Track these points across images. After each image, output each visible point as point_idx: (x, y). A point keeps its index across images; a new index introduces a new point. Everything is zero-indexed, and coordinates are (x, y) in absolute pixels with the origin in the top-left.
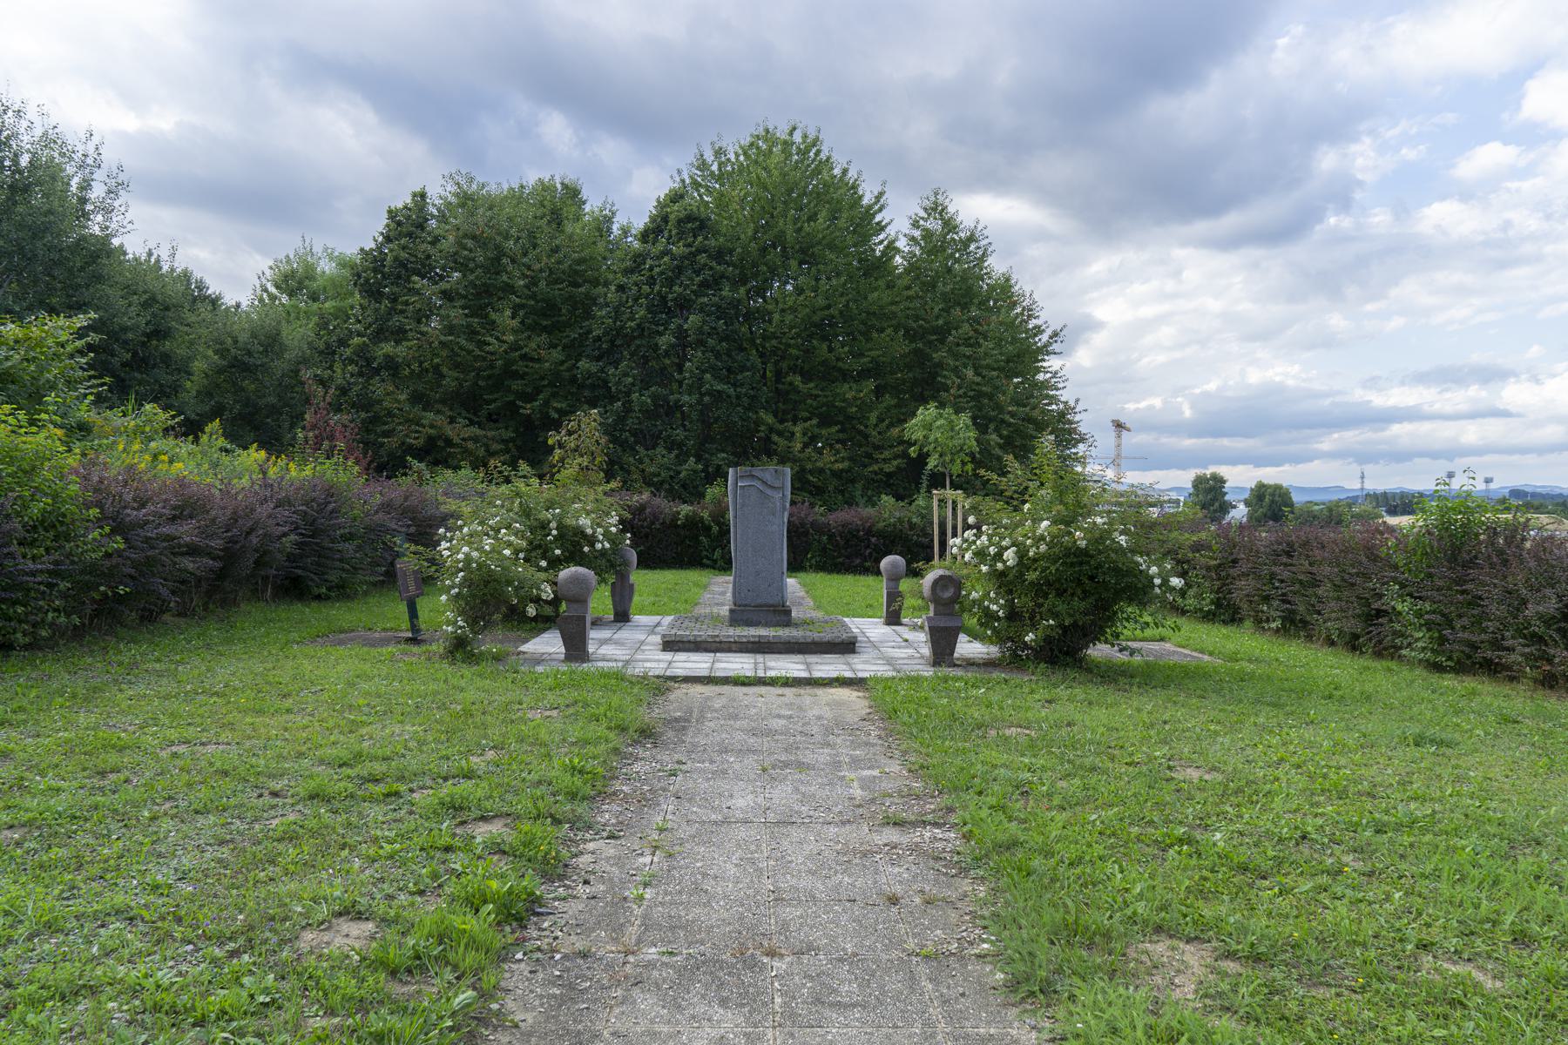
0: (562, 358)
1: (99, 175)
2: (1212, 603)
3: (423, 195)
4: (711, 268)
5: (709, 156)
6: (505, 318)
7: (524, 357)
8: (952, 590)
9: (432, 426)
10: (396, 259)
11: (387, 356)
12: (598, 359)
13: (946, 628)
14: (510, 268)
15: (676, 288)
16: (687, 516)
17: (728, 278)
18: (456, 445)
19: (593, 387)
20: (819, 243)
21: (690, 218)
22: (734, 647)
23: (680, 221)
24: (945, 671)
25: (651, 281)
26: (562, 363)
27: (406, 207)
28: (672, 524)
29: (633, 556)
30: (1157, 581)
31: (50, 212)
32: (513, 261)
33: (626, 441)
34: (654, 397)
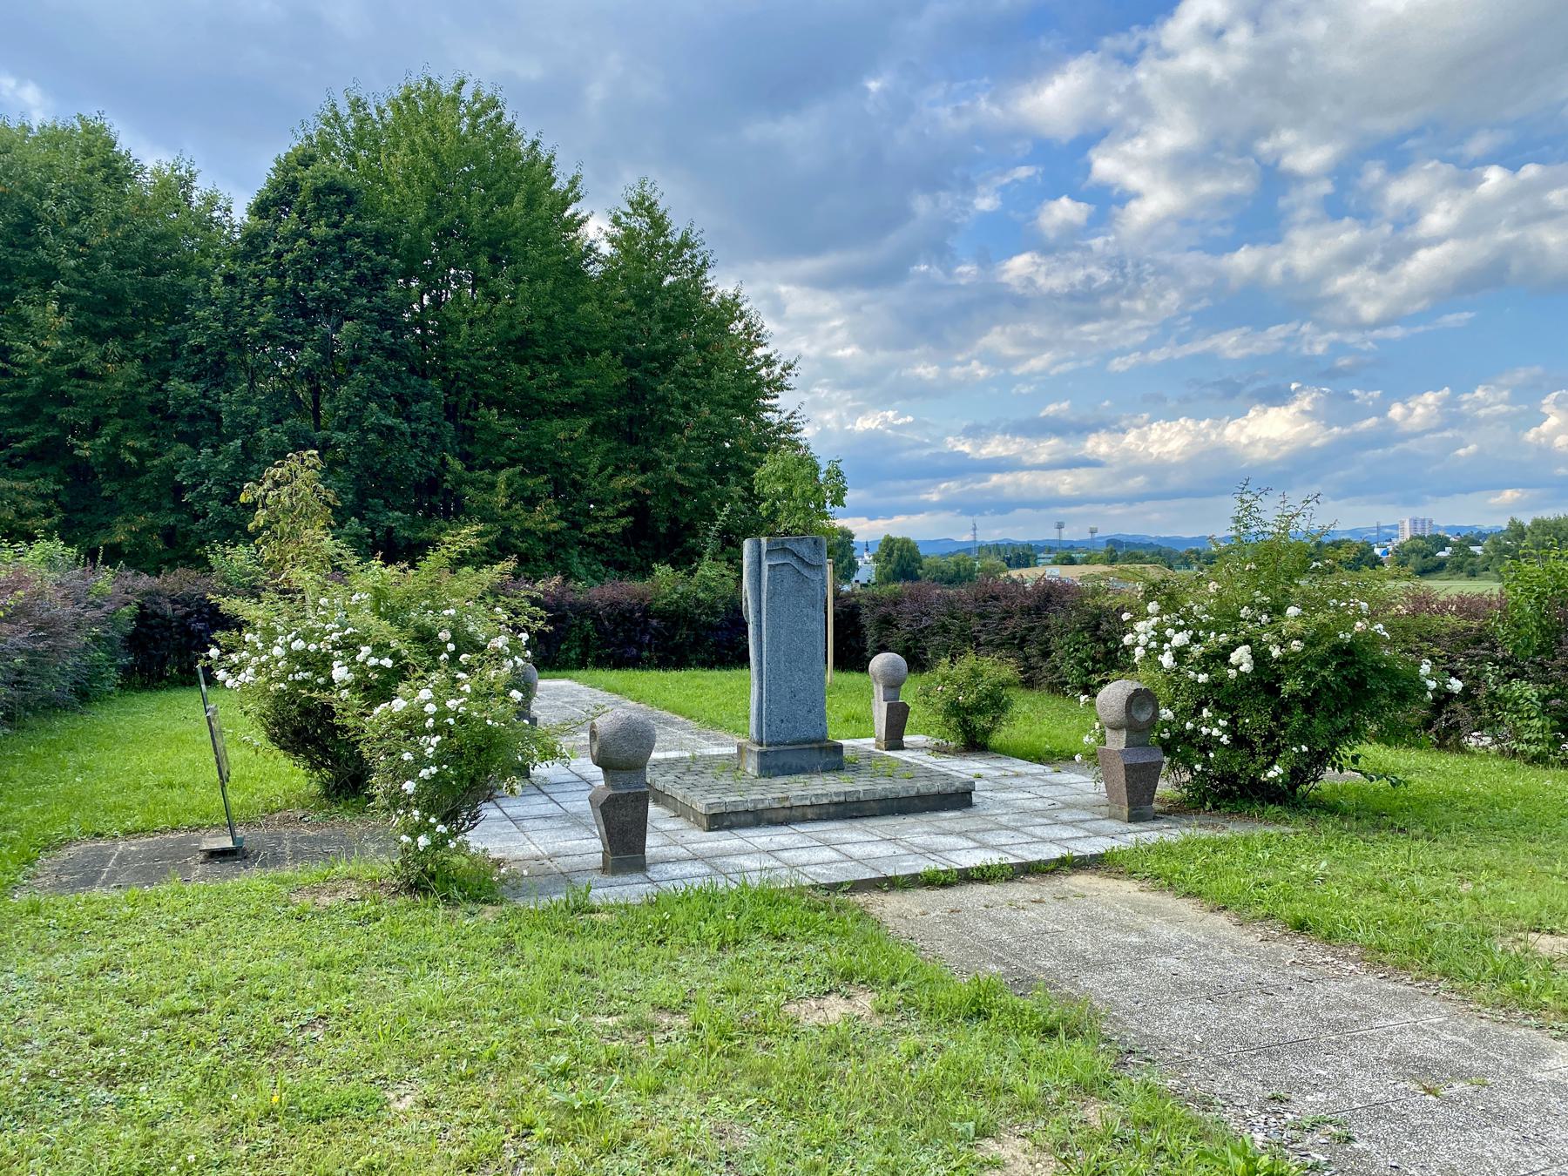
4: (369, 259)
5: (344, 110)
7: (82, 373)
12: (195, 379)
19: (192, 418)
20: (515, 235)
21: (332, 188)
22: (810, 813)
23: (317, 192)
26: (140, 383)
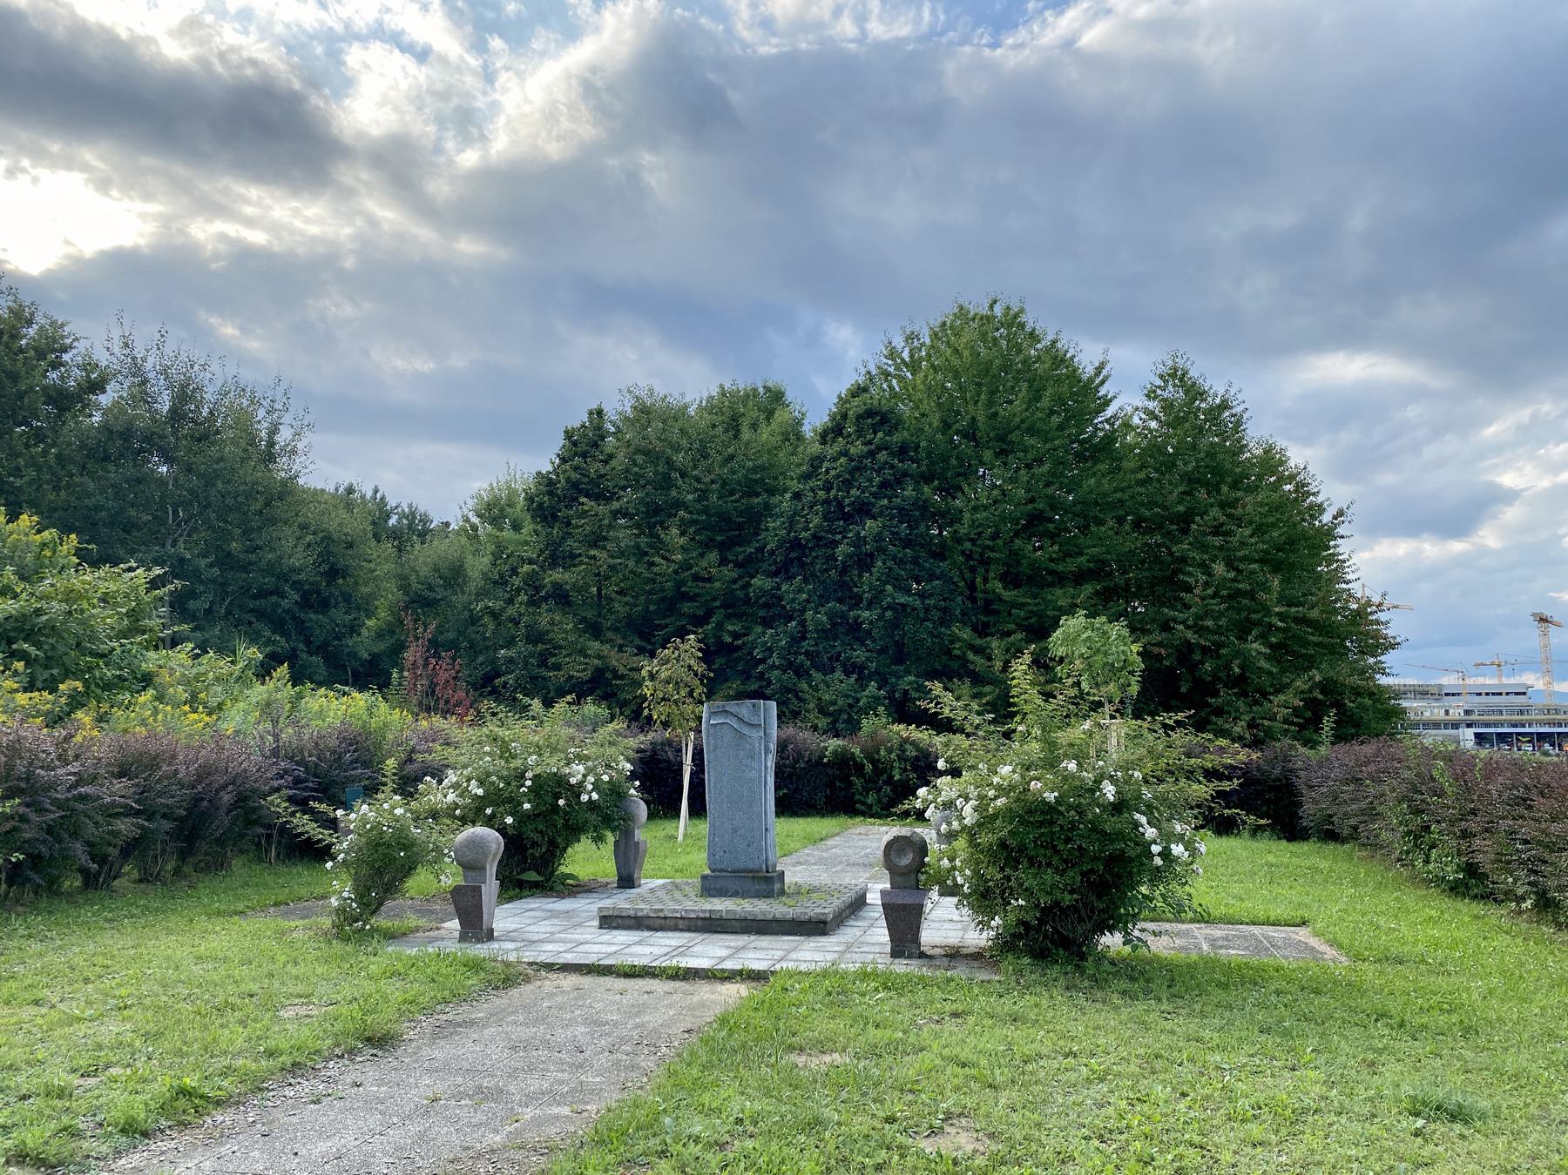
0: (735, 575)
1: (287, 418)
2: (1459, 869)
3: (600, 412)
4: (892, 467)
5: (899, 342)
6: (673, 536)
7: (696, 578)
8: (911, 856)
9: (599, 657)
10: (568, 480)
11: (554, 584)
12: (775, 574)
13: (904, 906)
14: (680, 482)
15: (853, 492)
16: (835, 752)
17: (911, 476)
18: (622, 677)
19: (767, 606)
20: (1018, 427)
21: (869, 413)
22: (681, 924)
23: (859, 417)
24: (902, 967)
25: (828, 487)
26: (734, 581)
27: (583, 426)
28: (817, 763)
29: (642, 810)
30: (1155, 849)
31: (222, 459)
32: (683, 476)
33: (802, 665)
34: (832, 615)
